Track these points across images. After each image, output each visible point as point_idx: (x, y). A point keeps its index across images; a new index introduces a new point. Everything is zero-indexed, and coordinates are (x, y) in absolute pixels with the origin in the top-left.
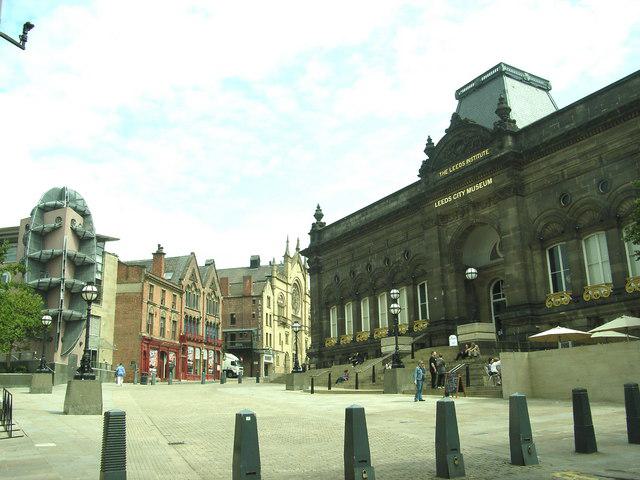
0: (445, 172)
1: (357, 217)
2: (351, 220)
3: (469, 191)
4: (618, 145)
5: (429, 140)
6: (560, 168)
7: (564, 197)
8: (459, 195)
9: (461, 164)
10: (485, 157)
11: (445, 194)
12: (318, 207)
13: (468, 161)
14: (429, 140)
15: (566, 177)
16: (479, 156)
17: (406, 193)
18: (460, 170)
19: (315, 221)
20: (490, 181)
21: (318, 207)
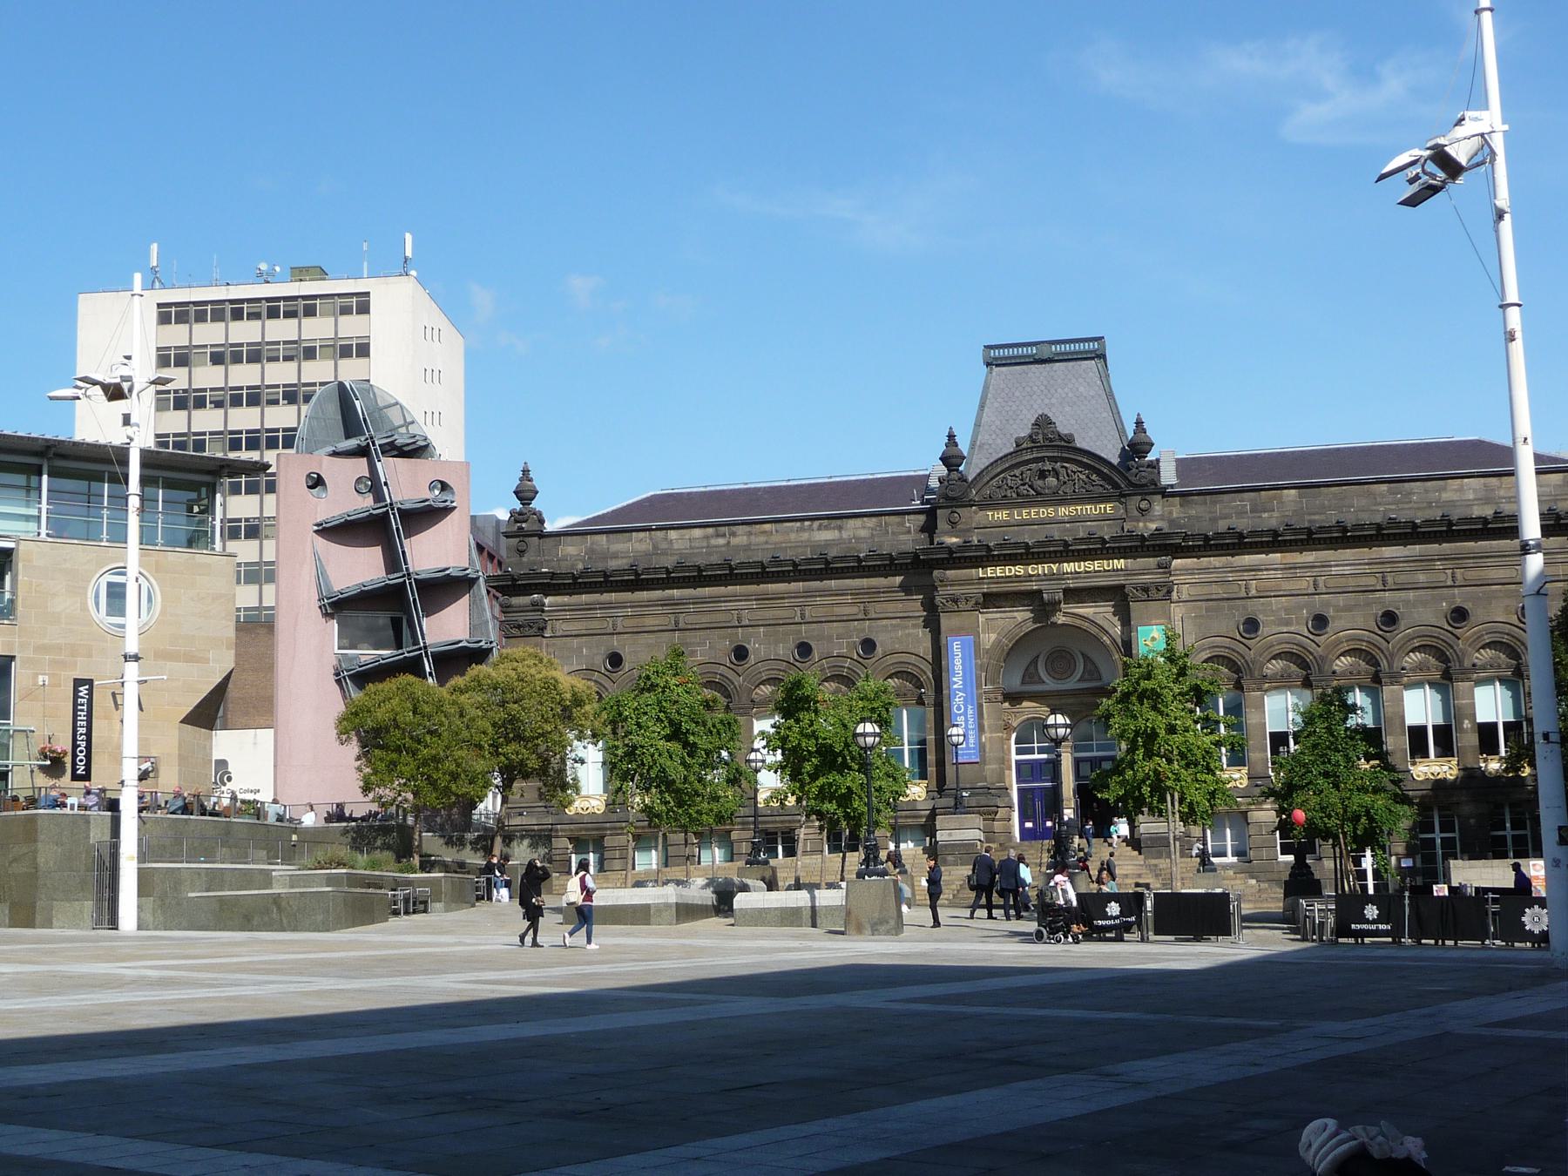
0: (1002, 515)
1: (697, 533)
2: (673, 534)
3: (1069, 567)
4: (1347, 570)
5: (951, 437)
6: (1246, 576)
7: (1252, 625)
8: (1041, 569)
9: (1045, 512)
10: (1105, 518)
11: (1012, 560)
12: (526, 472)
13: (1063, 511)
14: (951, 437)
15: (1253, 592)
16: (1089, 509)
18: (1042, 523)
19: (518, 505)
20: (1120, 564)
21: (526, 472)
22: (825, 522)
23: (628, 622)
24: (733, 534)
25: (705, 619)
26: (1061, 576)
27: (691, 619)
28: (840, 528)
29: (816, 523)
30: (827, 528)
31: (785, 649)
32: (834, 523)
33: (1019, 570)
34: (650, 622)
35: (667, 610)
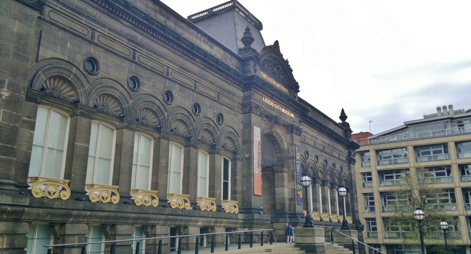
3: (283, 110)
8: (277, 107)
17: (222, 52)
20: (293, 116)
22: (206, 40)
23: (102, 39)
24: (168, 18)
25: (150, 64)
26: (281, 113)
27: (143, 60)
28: (211, 47)
29: (203, 38)
30: (207, 43)
31: (188, 104)
32: (210, 43)
33: (271, 103)
34: (117, 48)
35: (130, 44)
